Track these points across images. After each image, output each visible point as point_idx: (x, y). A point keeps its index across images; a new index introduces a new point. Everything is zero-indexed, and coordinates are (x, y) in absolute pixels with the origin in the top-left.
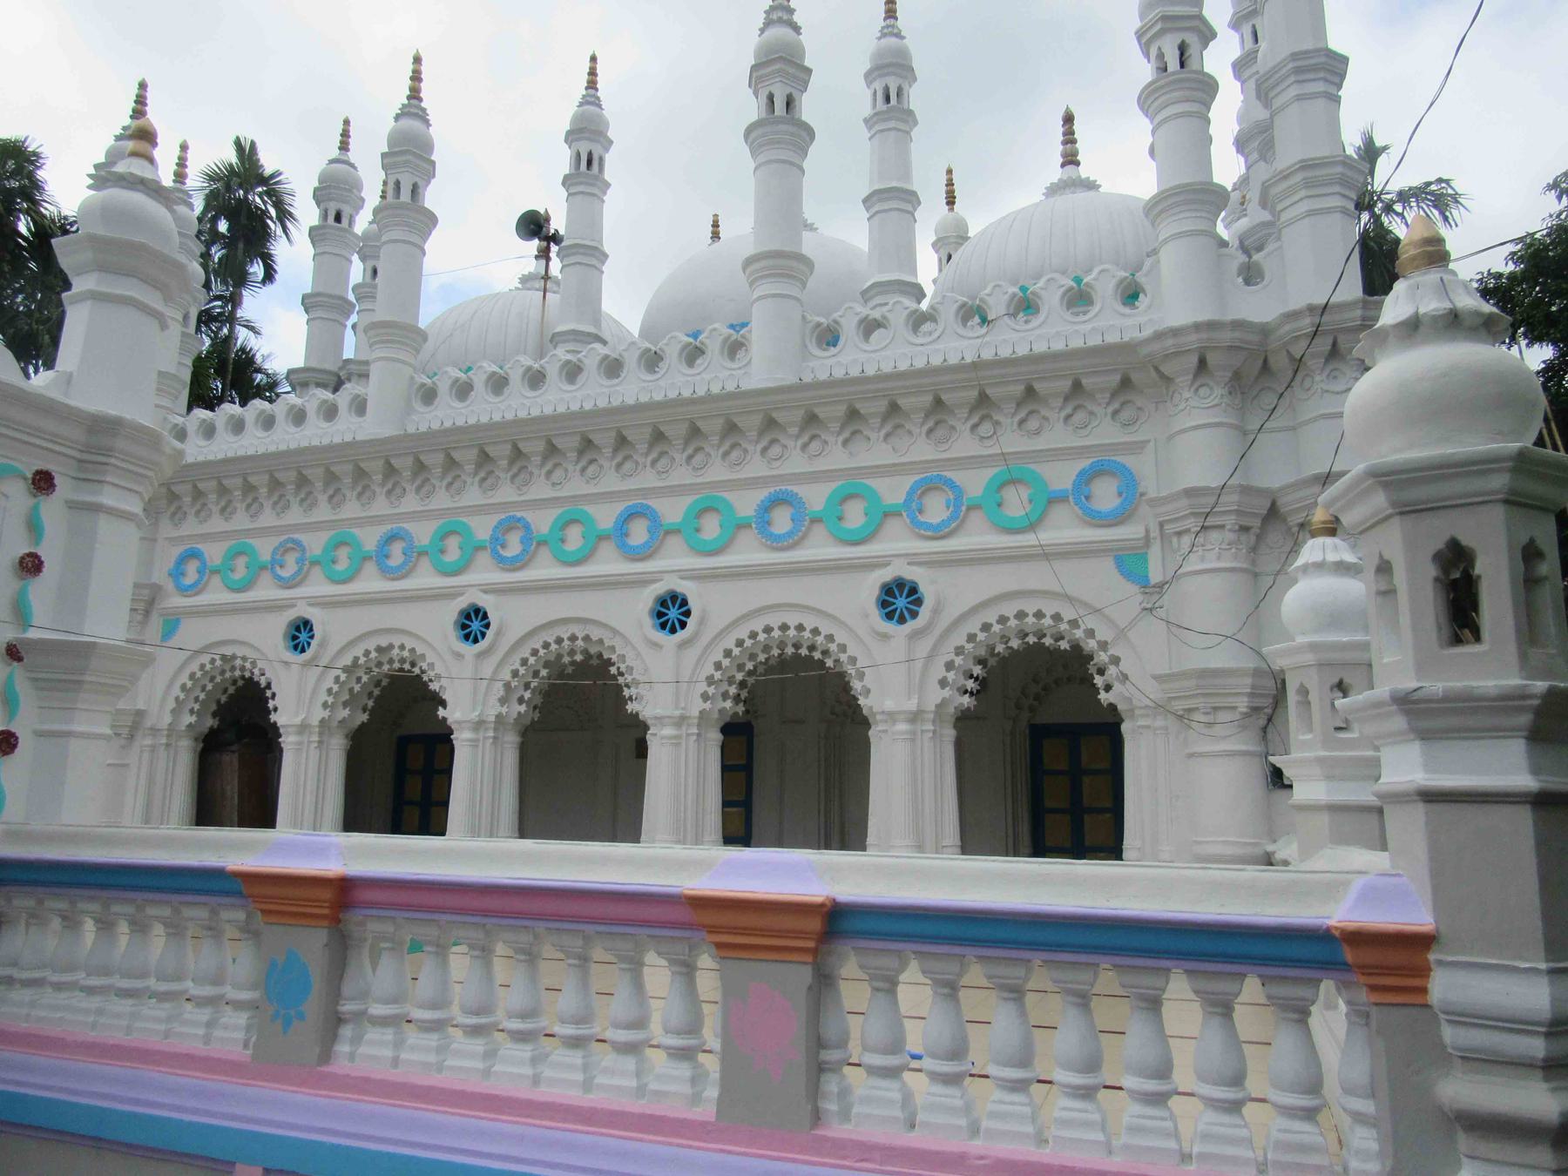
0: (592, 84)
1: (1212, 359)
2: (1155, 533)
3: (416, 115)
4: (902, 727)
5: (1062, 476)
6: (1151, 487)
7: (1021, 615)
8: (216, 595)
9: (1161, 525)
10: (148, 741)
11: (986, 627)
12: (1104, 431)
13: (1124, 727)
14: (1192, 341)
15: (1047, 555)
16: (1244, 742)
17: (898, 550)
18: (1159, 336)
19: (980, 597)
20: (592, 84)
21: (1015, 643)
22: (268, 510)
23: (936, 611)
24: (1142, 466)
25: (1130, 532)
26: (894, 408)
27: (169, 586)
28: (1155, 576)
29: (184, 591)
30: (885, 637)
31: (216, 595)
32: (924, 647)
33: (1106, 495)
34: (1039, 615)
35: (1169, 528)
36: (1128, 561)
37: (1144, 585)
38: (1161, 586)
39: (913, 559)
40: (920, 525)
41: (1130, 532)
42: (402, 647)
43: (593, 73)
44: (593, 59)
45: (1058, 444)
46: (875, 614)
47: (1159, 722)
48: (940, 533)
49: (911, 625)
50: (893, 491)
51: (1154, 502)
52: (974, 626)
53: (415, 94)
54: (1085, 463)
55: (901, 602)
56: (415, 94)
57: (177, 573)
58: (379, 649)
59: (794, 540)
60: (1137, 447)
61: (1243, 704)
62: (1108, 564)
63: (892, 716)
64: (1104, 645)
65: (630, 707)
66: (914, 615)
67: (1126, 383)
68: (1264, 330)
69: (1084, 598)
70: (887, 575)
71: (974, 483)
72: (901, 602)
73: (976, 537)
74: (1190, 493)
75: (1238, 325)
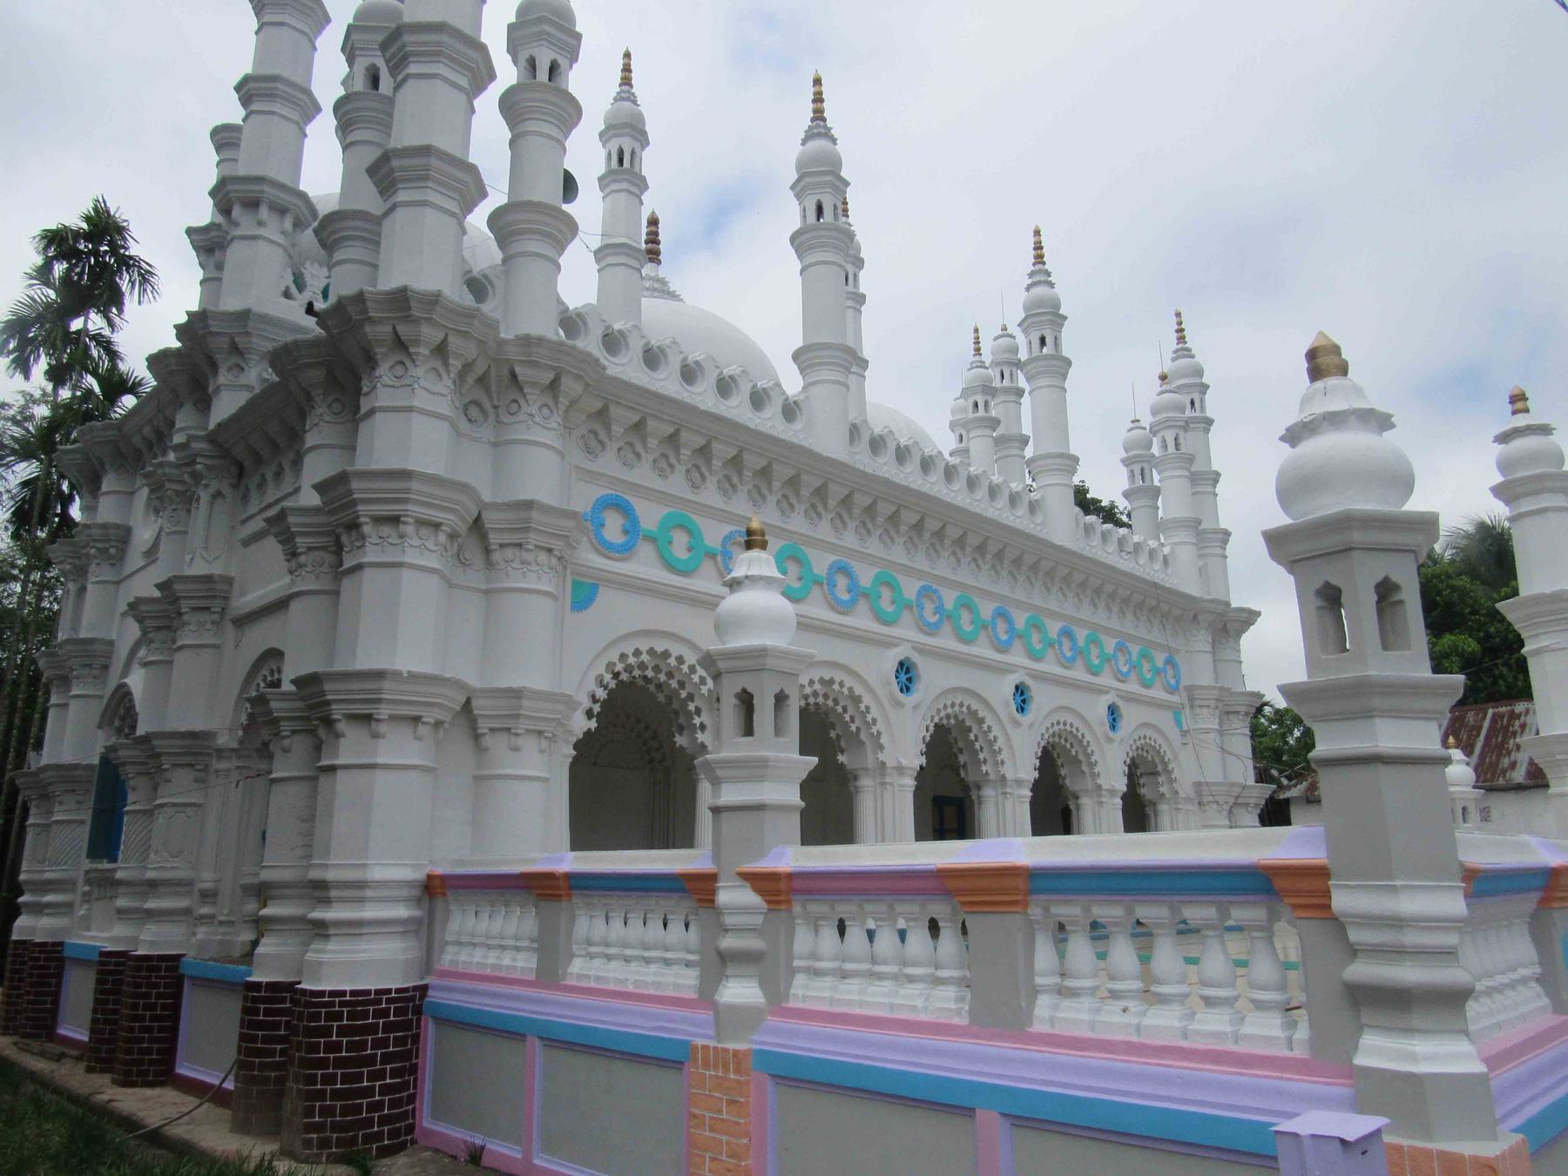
0: (626, 81)
2: (1186, 701)
3: (819, 135)
8: (644, 566)
9: (1191, 699)
18: (1212, 601)
20: (626, 81)
24: (1178, 659)
29: (605, 549)
31: (644, 566)
35: (1197, 703)
42: (841, 684)
43: (627, 69)
44: (627, 55)
47: (1190, 807)
53: (819, 115)
56: (819, 115)
58: (822, 681)
59: (1067, 664)
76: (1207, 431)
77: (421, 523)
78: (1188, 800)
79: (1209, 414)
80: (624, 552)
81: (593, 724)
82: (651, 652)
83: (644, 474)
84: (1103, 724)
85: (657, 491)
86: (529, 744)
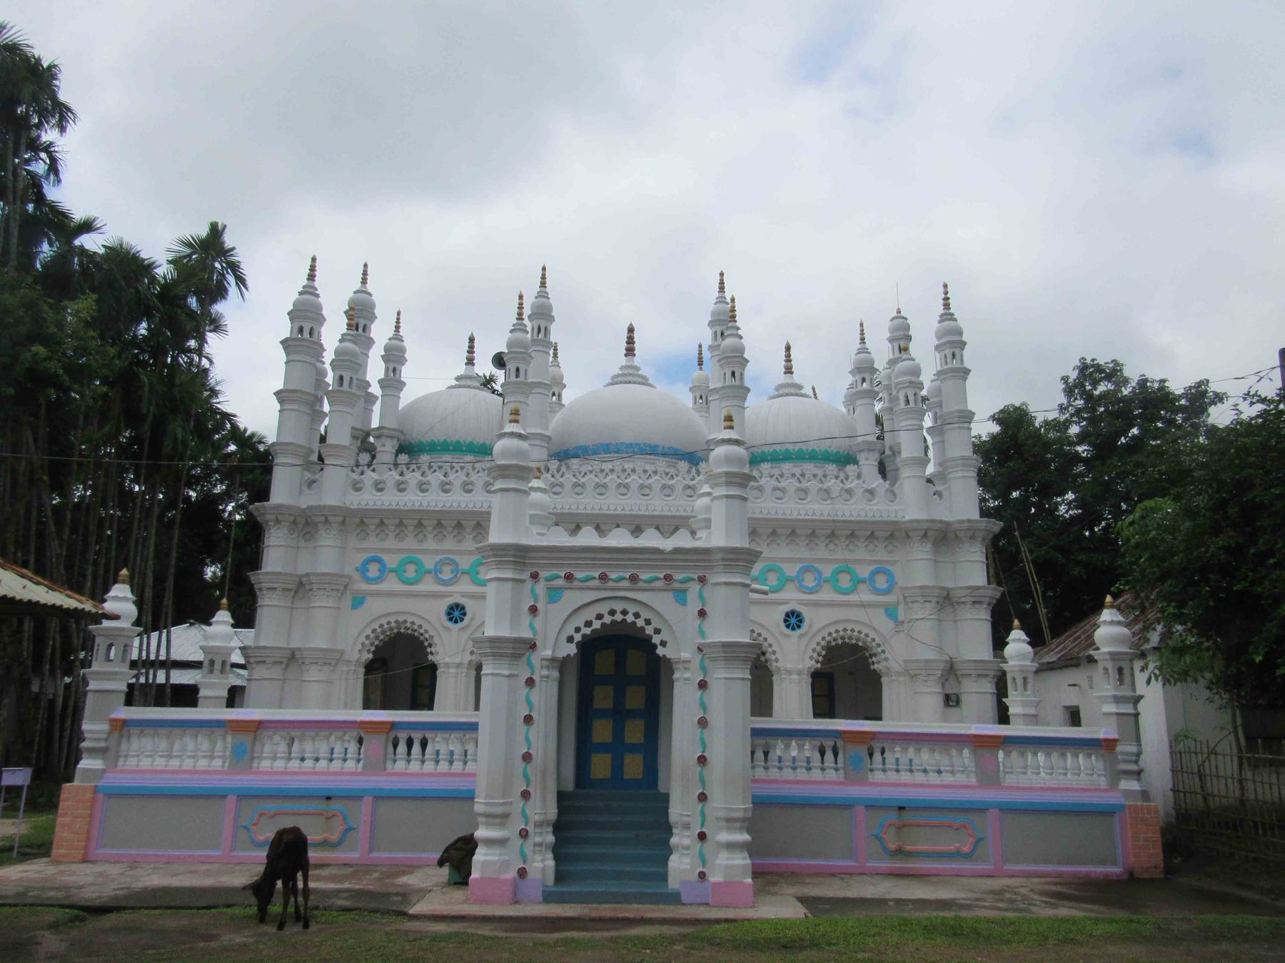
1: (930, 533)
4: (795, 677)
5: (864, 572)
6: (901, 582)
7: (845, 630)
8: (391, 584)
9: (905, 597)
10: (345, 668)
11: (830, 634)
12: (881, 554)
13: (884, 680)
14: (924, 526)
15: (863, 605)
16: (937, 689)
17: (792, 597)
18: (912, 521)
19: (824, 622)
21: (840, 642)
22: (430, 536)
23: (810, 626)
24: (896, 570)
25: (891, 598)
26: (793, 533)
27: (357, 576)
28: (901, 618)
29: (369, 581)
30: (787, 636)
32: (806, 639)
33: (881, 582)
34: (860, 632)
35: (909, 599)
36: (890, 612)
37: (896, 621)
38: (902, 622)
39: (801, 602)
40: (803, 587)
41: (891, 598)
45: (864, 557)
46: (783, 625)
47: (902, 679)
48: (812, 591)
49: (798, 632)
50: (792, 570)
51: (903, 588)
52: (825, 633)
54: (873, 567)
55: (793, 620)
57: (363, 569)
60: (894, 563)
61: (939, 673)
62: (882, 611)
63: (789, 672)
64: (879, 645)
65: (430, 657)
66: (799, 627)
67: (892, 535)
68: (948, 524)
69: (871, 625)
70: (788, 608)
71: (827, 570)
72: (793, 620)
73: (826, 595)
74: (921, 587)
75: (941, 522)
76: (965, 379)
77: (269, 589)
78: (899, 673)
79: (967, 364)
80: (378, 580)
81: (371, 656)
82: (397, 622)
83: (391, 543)
84: (778, 625)
85: (392, 549)
86: (314, 667)
